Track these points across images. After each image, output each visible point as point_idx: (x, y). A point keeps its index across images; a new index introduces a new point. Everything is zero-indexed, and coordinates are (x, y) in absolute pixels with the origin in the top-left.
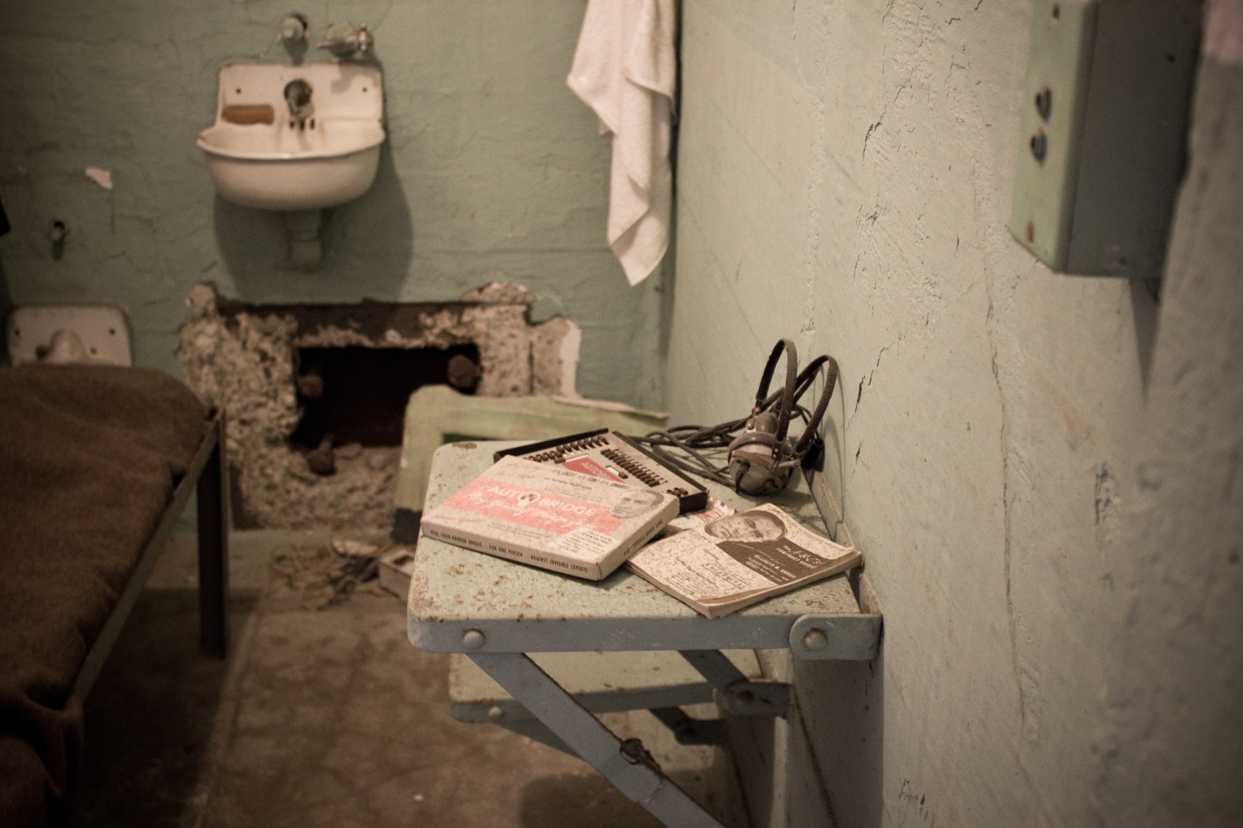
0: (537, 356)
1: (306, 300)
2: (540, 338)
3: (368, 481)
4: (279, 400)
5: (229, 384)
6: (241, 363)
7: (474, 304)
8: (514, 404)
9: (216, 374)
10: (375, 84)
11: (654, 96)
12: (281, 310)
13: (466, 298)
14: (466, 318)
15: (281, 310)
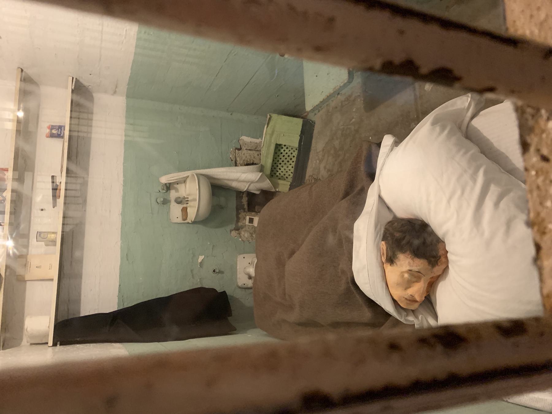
0: (249, 148)
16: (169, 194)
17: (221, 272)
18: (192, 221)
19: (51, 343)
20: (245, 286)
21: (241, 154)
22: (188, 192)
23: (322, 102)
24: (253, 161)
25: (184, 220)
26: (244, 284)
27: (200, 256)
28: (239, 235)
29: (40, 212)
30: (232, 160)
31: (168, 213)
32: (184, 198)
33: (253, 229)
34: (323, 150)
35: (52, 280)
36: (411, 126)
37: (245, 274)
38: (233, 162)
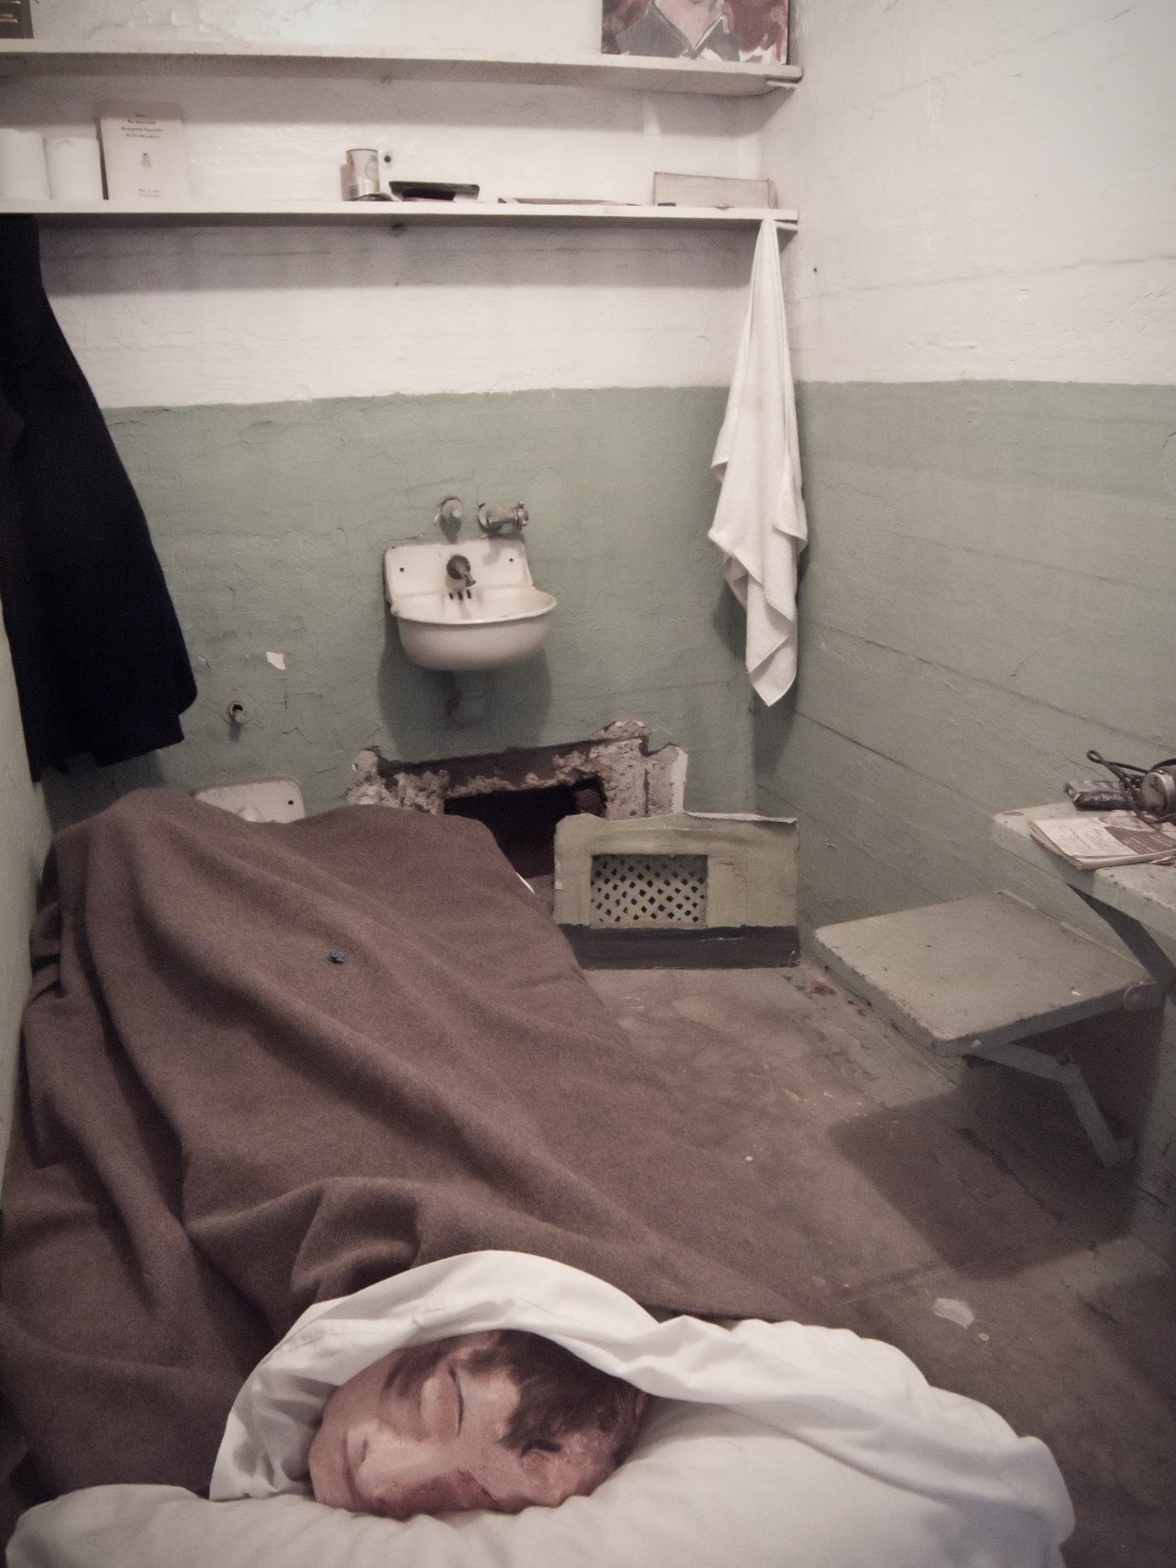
0: (651, 781)
1: (458, 754)
2: (654, 765)
8: (634, 824)
11: (794, 540)
12: (434, 766)
13: (593, 738)
14: (592, 755)
15: (434, 766)
16: (473, 538)
17: (236, 728)
24: (613, 800)
27: (281, 656)
31: (415, 540)
32: (470, 582)
34: (681, 1020)
35: (106, 196)
38: (603, 731)
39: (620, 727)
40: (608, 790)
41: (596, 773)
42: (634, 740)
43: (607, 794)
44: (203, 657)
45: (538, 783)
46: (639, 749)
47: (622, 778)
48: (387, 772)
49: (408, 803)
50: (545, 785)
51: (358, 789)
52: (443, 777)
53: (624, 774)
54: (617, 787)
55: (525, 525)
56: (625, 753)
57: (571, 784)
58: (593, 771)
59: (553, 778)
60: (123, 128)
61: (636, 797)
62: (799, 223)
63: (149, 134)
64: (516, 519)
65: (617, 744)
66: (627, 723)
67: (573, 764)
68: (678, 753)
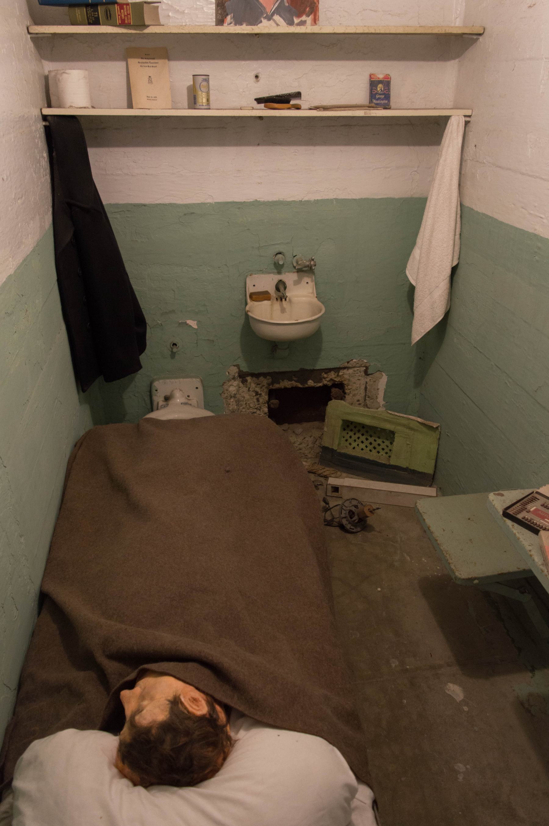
0: (368, 387)
1: (277, 370)
2: (370, 380)
3: (296, 440)
4: (261, 410)
5: (242, 405)
6: (247, 397)
7: (344, 368)
9: (236, 401)
10: (312, 281)
12: (265, 375)
13: (341, 366)
14: (340, 374)
15: (265, 375)
17: (173, 355)
18: (248, 311)
19: (47, 111)
20: (154, 391)
21: (359, 376)
22: (295, 299)
23: (429, 529)
24: (349, 394)
25: (252, 296)
26: (156, 390)
28: (232, 377)
29: (253, 74)
30: (348, 362)
31: (262, 272)
33: (242, 399)
36: (394, 660)
37: (173, 391)
38: (346, 363)
39: (355, 362)
40: (347, 390)
41: (342, 381)
42: (361, 368)
43: (346, 391)
44: (159, 321)
45: (314, 385)
46: (364, 372)
47: (354, 384)
48: (242, 376)
49: (252, 390)
50: (317, 386)
51: (229, 383)
52: (269, 379)
53: (355, 383)
54: (351, 388)
55: (314, 269)
56: (357, 373)
57: (329, 385)
58: (340, 380)
59: (320, 383)
60: (139, 62)
61: (360, 393)
62: (472, 117)
63: (151, 65)
64: (310, 266)
65: (353, 369)
66: (358, 360)
67: (331, 377)
68: (383, 375)
